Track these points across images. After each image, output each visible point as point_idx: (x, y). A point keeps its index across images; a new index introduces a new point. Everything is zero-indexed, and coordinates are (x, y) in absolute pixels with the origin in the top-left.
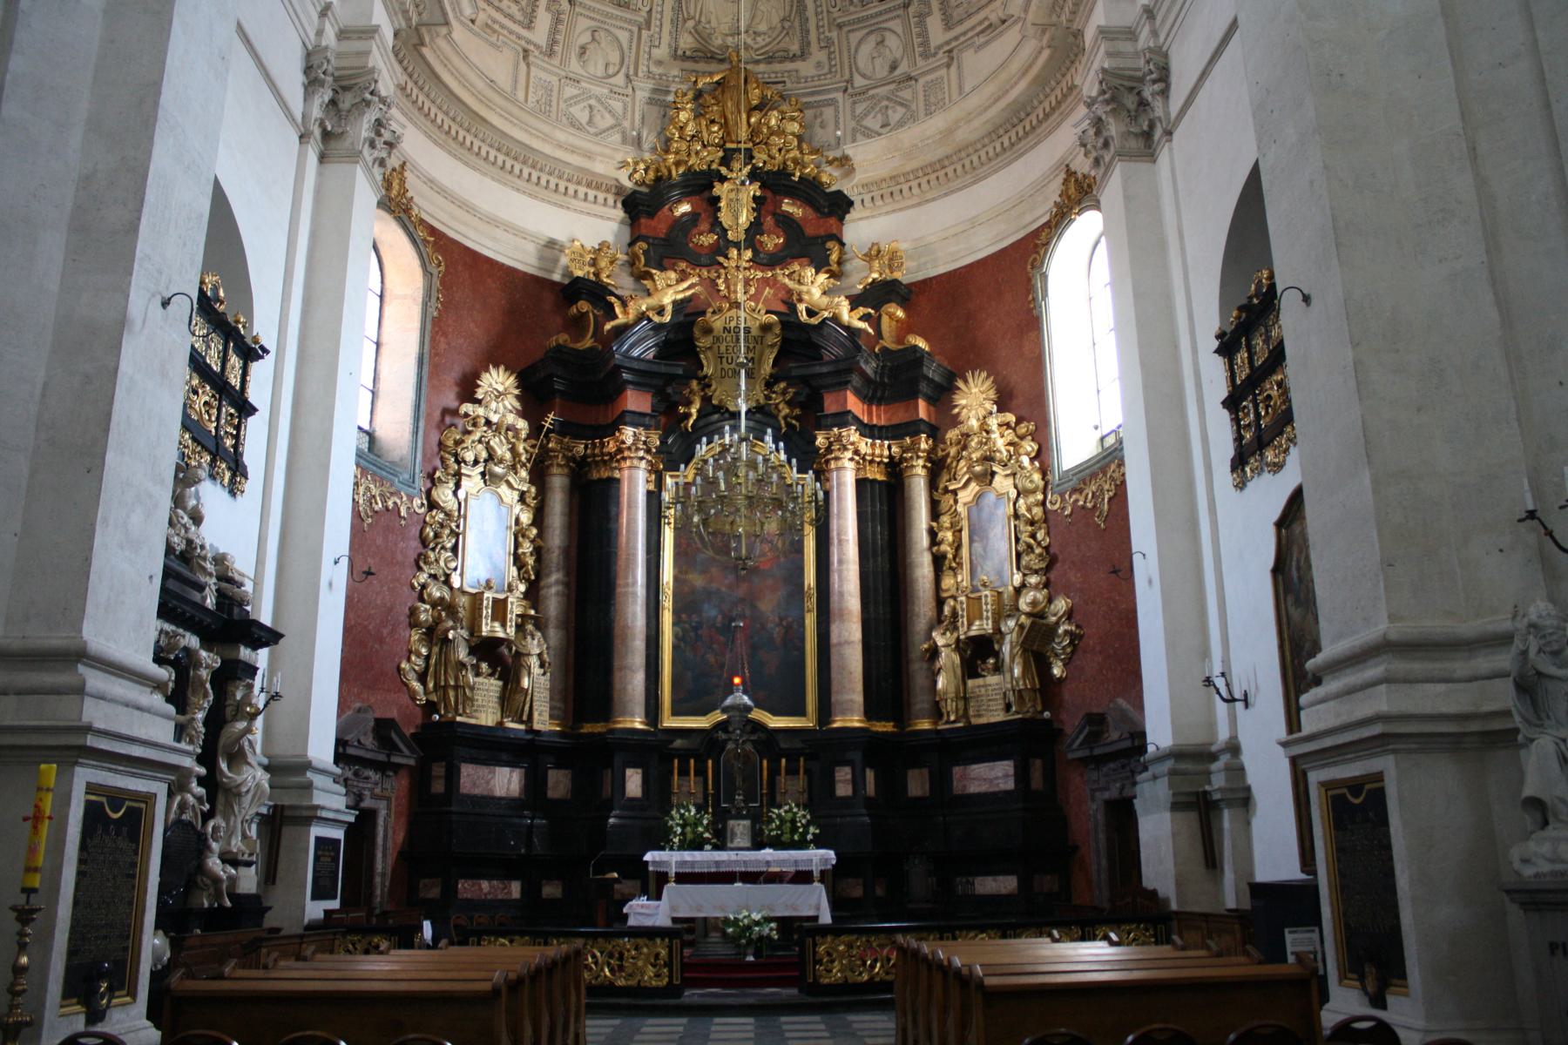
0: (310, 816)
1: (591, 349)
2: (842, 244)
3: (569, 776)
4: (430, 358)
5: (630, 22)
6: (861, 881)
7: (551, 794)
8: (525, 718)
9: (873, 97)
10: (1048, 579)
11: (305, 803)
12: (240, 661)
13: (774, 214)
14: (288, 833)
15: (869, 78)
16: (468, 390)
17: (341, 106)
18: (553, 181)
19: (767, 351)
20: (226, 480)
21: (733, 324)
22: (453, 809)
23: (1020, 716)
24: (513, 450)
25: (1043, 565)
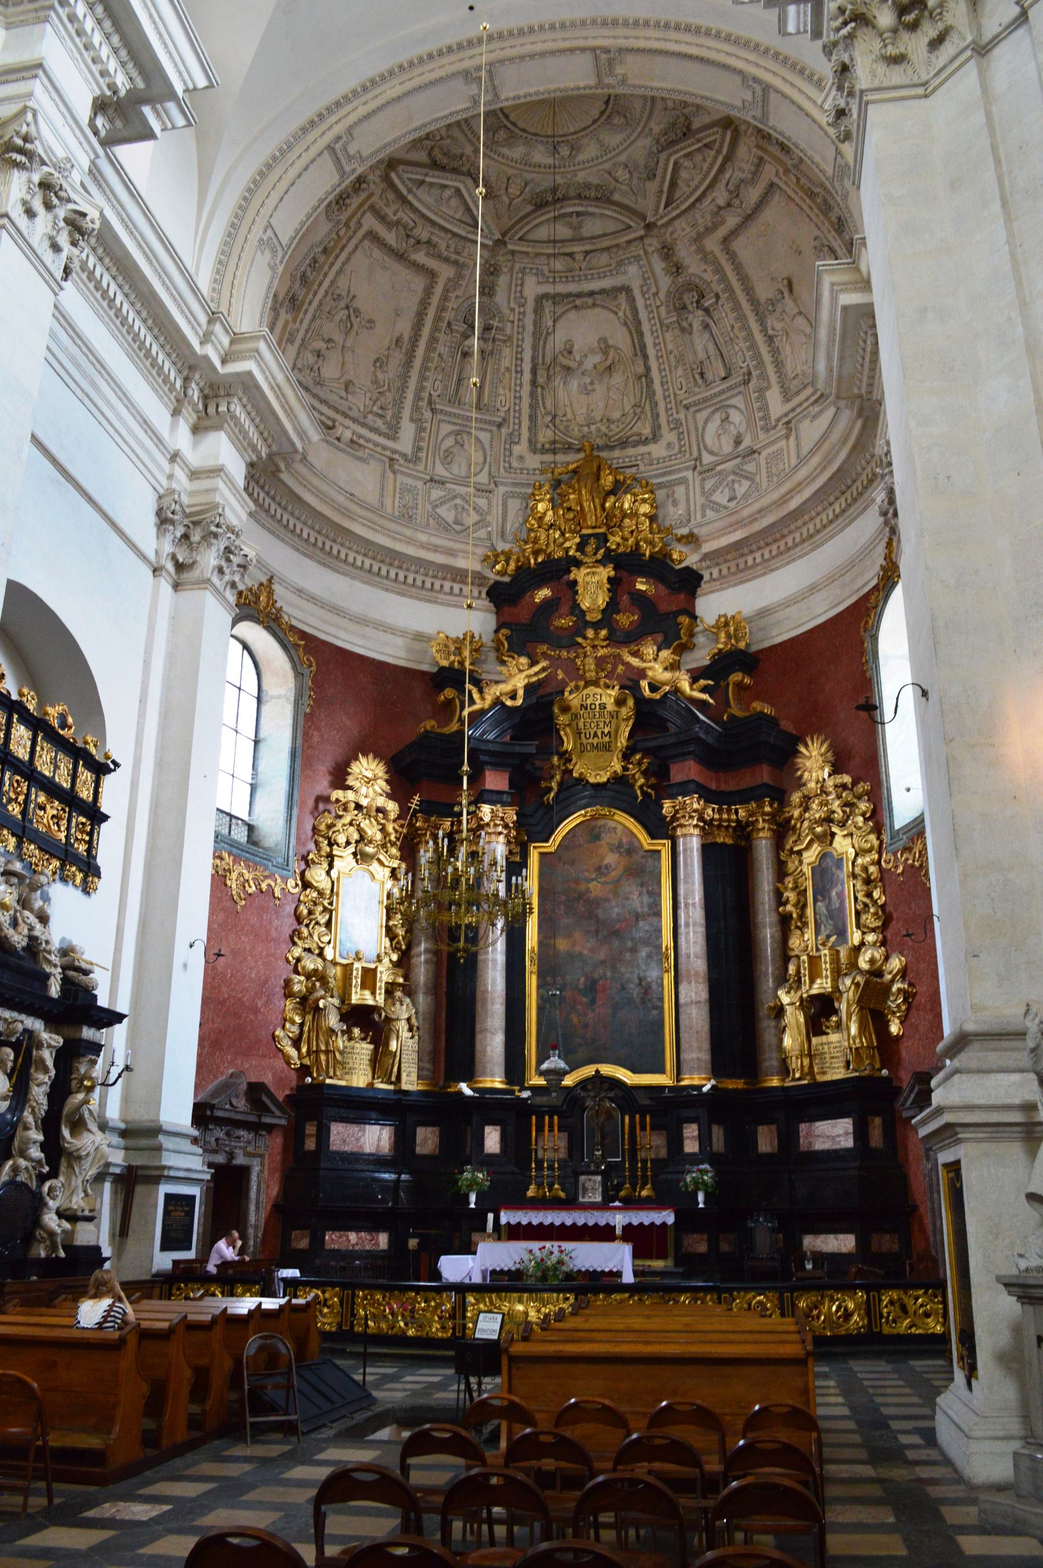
0: (156, 1176)
2: (694, 617)
5: (490, 423)
6: (705, 1236)
7: (419, 1150)
8: (393, 1079)
9: (720, 473)
10: (884, 937)
11: (156, 1164)
12: (81, 1040)
14: (140, 1190)
16: (340, 778)
17: (192, 539)
19: (623, 724)
20: (78, 881)
21: (589, 702)
22: (323, 1165)
24: (383, 830)
25: (879, 923)
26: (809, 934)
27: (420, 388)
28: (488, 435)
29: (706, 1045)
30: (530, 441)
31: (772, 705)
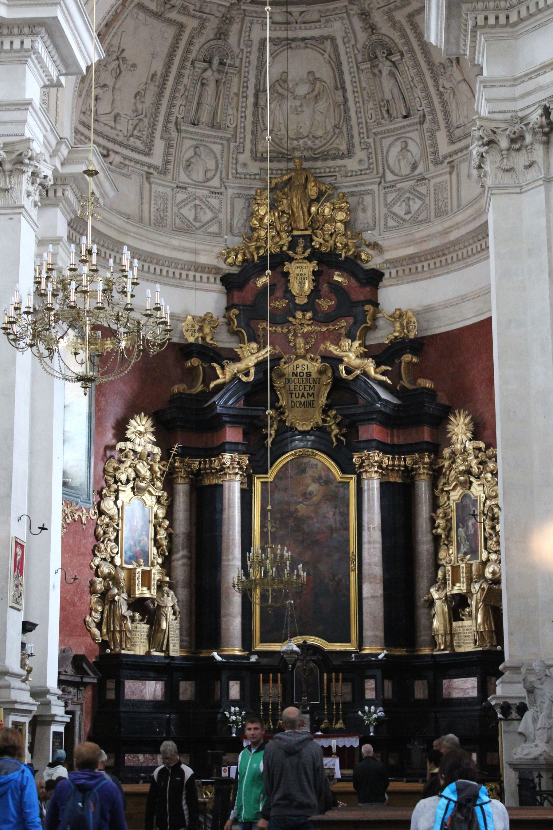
0: (51, 720)
1: (202, 392)
2: (376, 304)
3: (194, 685)
4: (96, 413)
5: (221, 138)
7: (181, 697)
8: (164, 649)
9: (399, 189)
13: (328, 283)
14: (38, 729)
15: (396, 175)
16: (121, 435)
18: (171, 270)
21: (299, 370)
22: (122, 709)
23: (481, 649)
24: (151, 469)
26: (452, 550)
27: (169, 114)
28: (220, 147)
29: (381, 626)
30: (252, 151)
31: (432, 379)
